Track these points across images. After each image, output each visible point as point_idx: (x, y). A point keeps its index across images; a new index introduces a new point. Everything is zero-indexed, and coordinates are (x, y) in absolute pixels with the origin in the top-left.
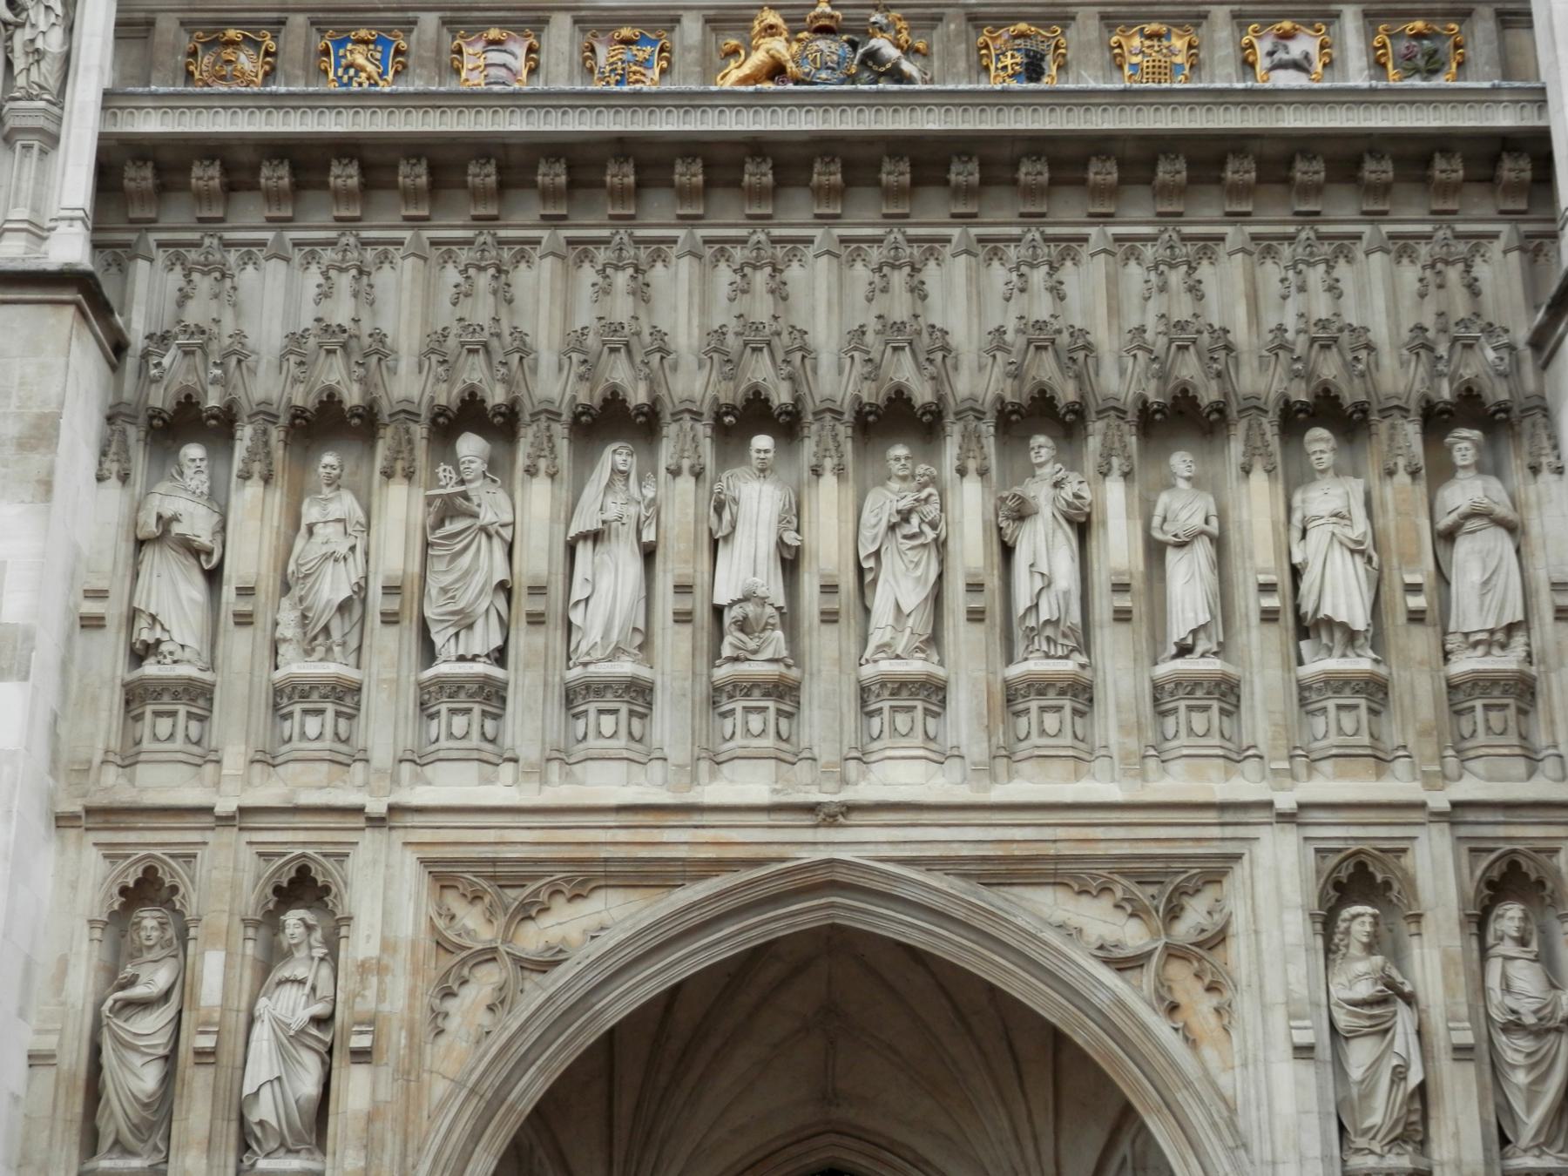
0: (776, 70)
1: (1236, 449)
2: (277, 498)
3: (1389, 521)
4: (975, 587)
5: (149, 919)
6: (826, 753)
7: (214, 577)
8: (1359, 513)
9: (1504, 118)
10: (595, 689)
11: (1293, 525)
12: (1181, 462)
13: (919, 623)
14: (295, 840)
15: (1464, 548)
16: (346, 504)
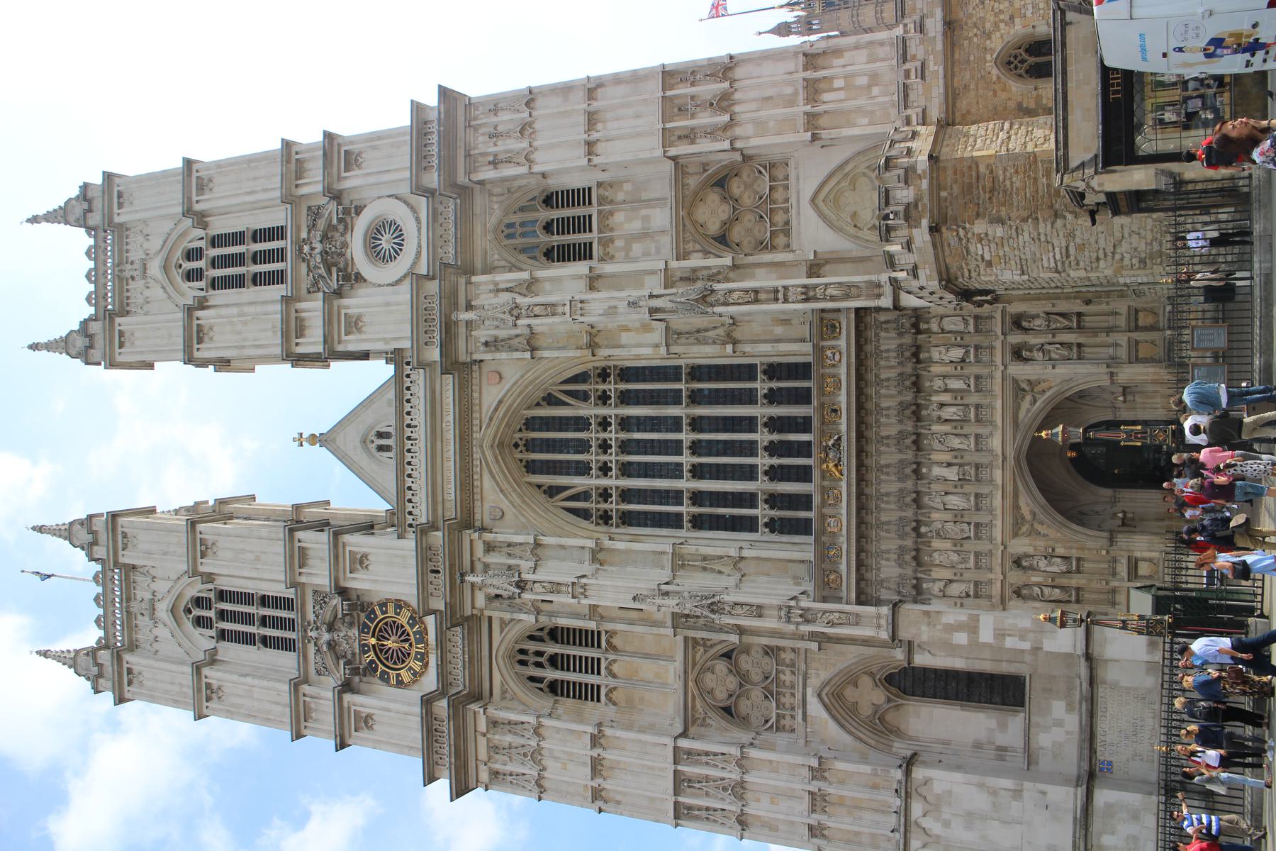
0: (836, 466)
1: (924, 373)
2: (934, 569)
3: (940, 342)
4: (956, 428)
5: (1024, 592)
6: (991, 458)
7: (951, 581)
8: (938, 349)
9: (853, 316)
10: (977, 504)
11: (941, 362)
12: (927, 384)
13: (963, 439)
14: (1008, 564)
15: (947, 328)
16: (936, 555)
